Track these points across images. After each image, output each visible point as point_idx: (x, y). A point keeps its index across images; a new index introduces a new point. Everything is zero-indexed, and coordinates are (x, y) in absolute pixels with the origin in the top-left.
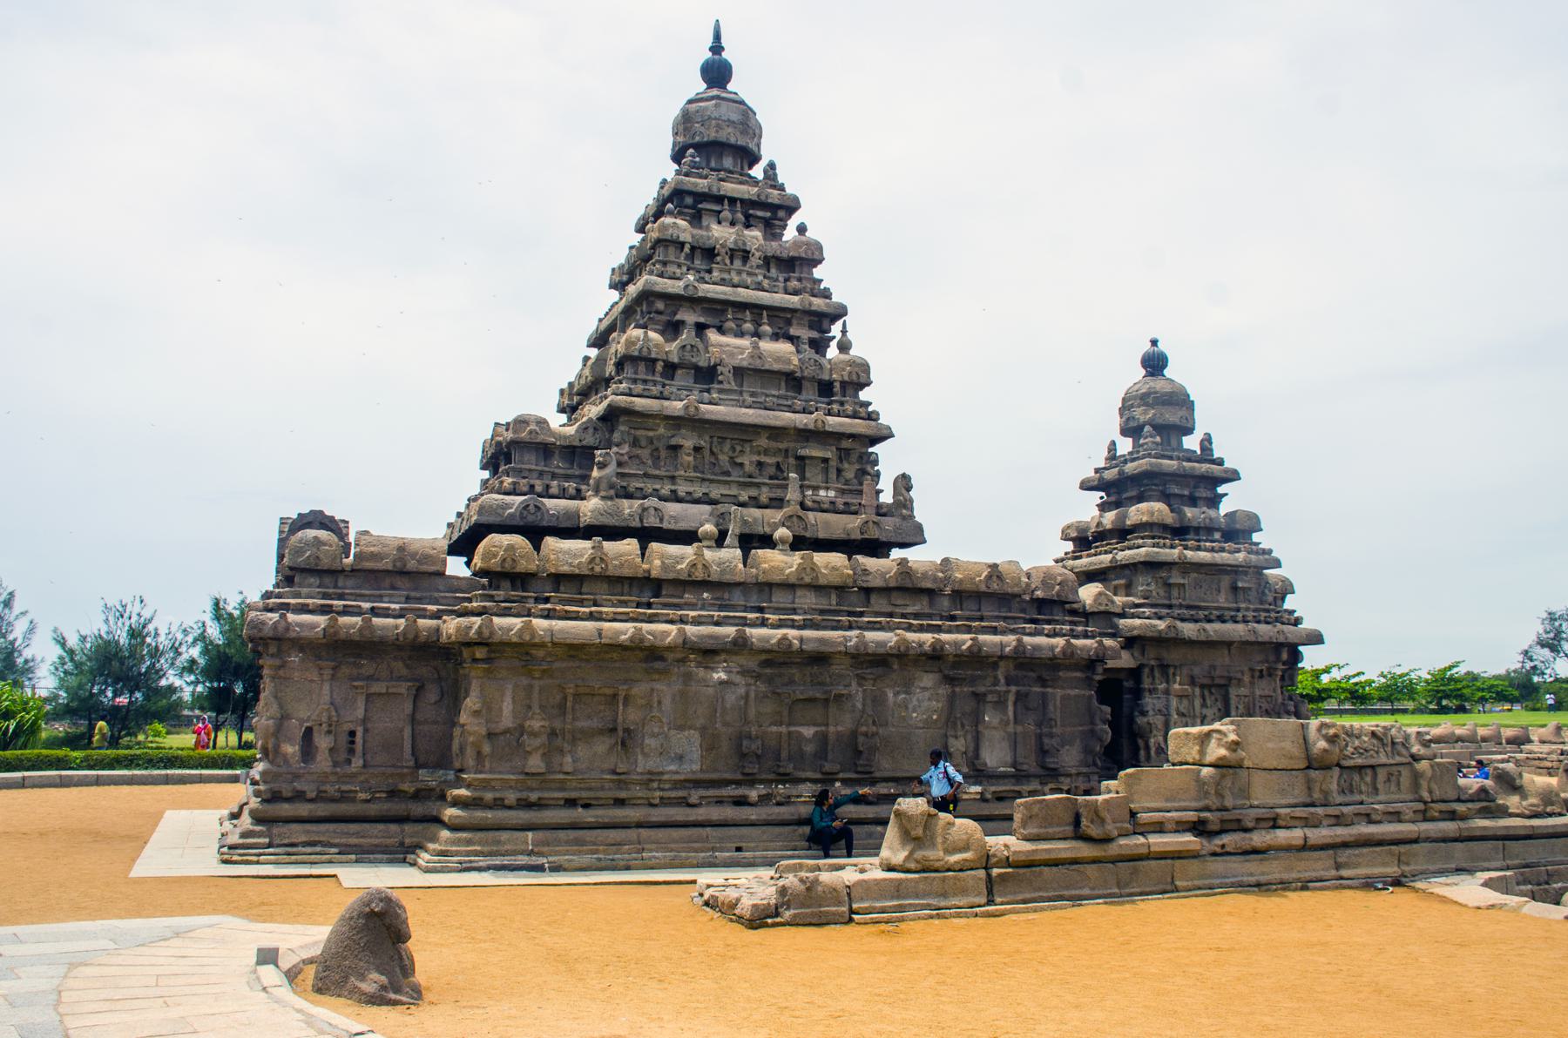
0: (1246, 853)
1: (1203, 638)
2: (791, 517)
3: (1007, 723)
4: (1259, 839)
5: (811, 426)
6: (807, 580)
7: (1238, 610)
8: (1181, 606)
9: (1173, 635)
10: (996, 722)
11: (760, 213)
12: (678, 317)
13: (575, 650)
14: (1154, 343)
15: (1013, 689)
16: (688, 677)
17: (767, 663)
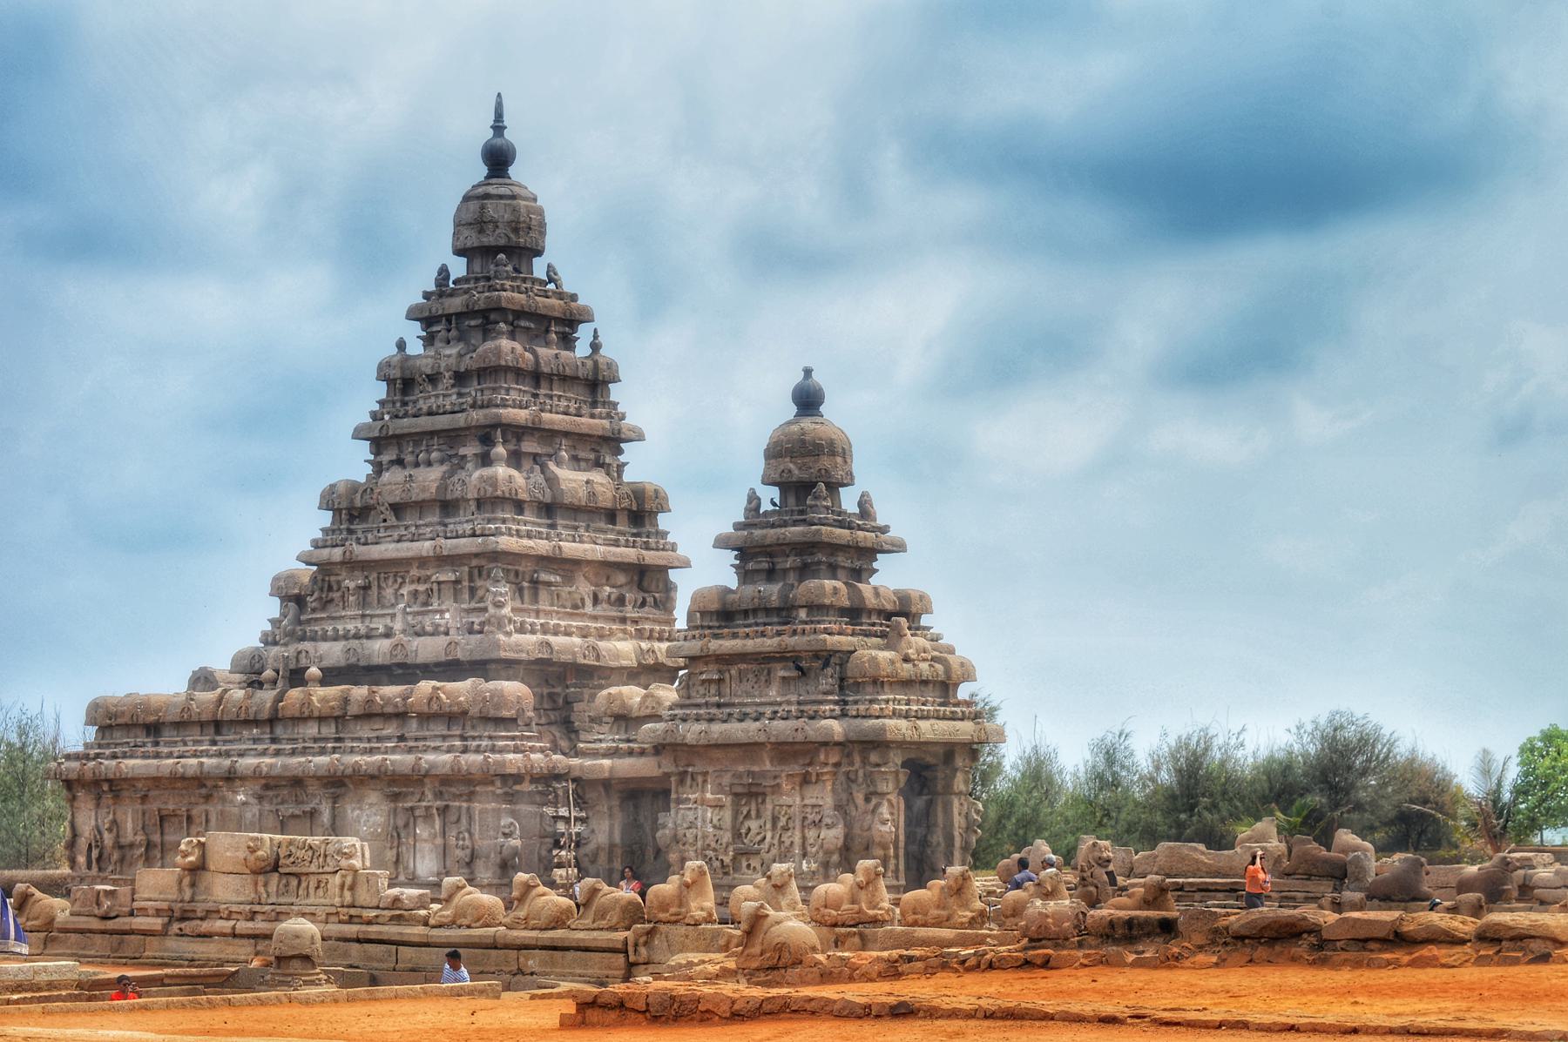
0: (199, 936)
1: (702, 742)
2: (397, 645)
3: (435, 836)
4: (205, 926)
5: (431, 554)
6: (306, 714)
7: (780, 704)
8: (707, 704)
9: (673, 741)
10: (425, 835)
11: (473, 323)
12: (379, 459)
13: (156, 781)
14: (808, 372)
15: (438, 803)
16: (223, 800)
17: (267, 787)
